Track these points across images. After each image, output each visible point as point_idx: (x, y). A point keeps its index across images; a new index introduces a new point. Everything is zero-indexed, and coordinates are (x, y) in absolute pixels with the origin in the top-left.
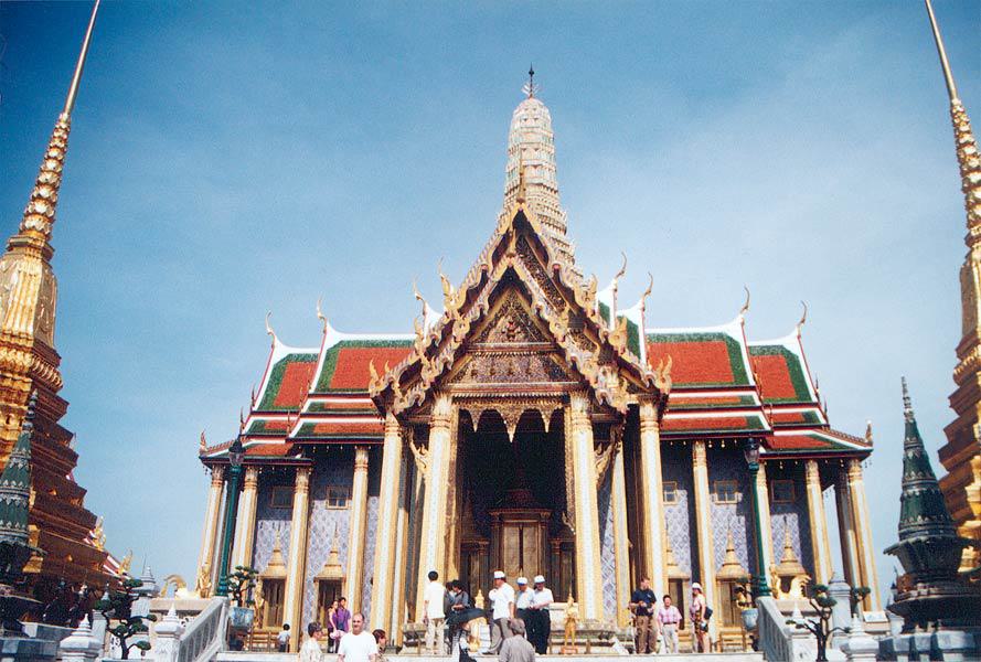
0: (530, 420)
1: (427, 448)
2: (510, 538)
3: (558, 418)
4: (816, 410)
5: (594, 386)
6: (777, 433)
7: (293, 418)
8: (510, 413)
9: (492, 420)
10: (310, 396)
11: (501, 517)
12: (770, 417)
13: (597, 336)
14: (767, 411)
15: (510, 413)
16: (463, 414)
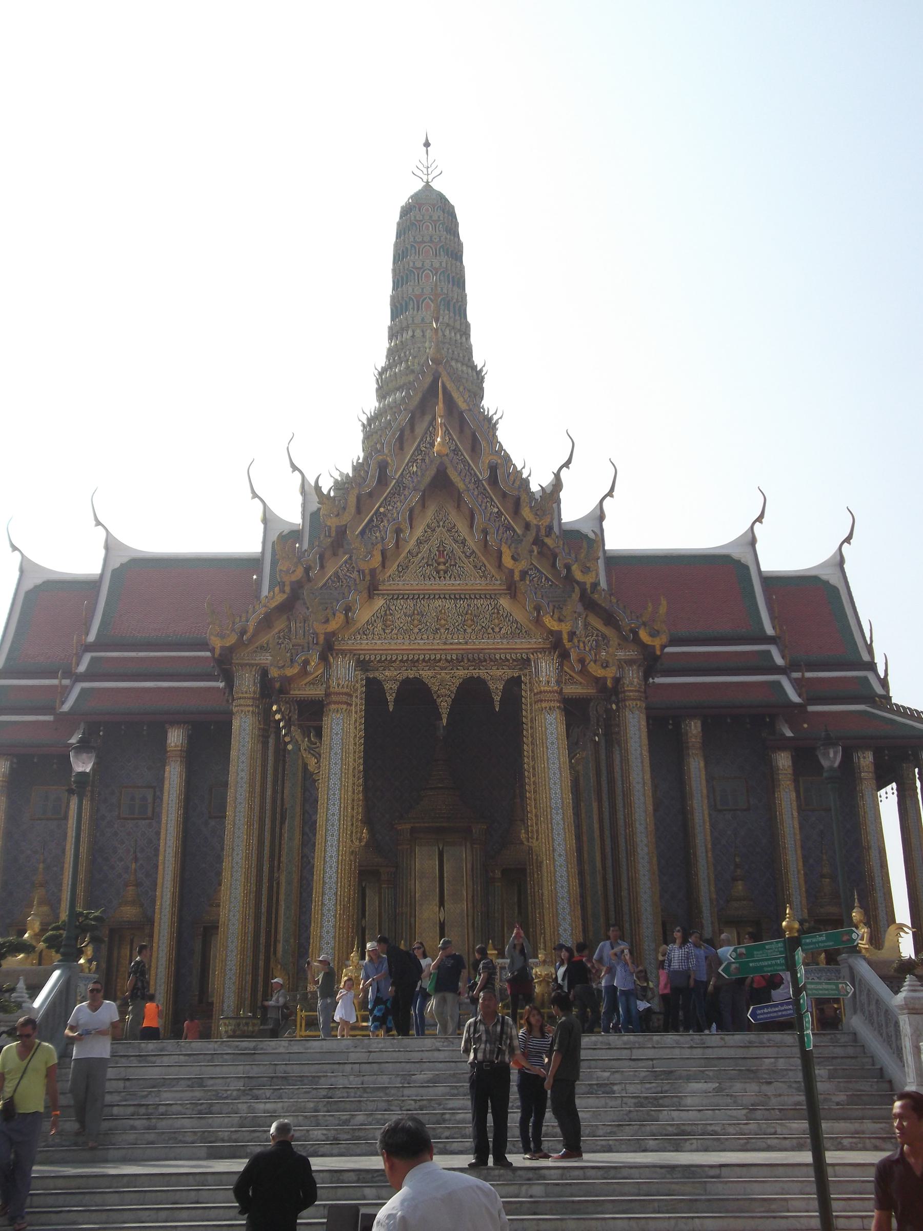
0: (472, 692)
1: (319, 735)
2: (424, 862)
3: (514, 684)
4: (870, 675)
5: (568, 645)
6: (811, 708)
7: (66, 682)
8: (444, 684)
9: (415, 693)
10: (88, 648)
11: (413, 830)
12: (797, 684)
13: (554, 565)
14: (796, 675)
15: (444, 684)
16: (374, 689)
